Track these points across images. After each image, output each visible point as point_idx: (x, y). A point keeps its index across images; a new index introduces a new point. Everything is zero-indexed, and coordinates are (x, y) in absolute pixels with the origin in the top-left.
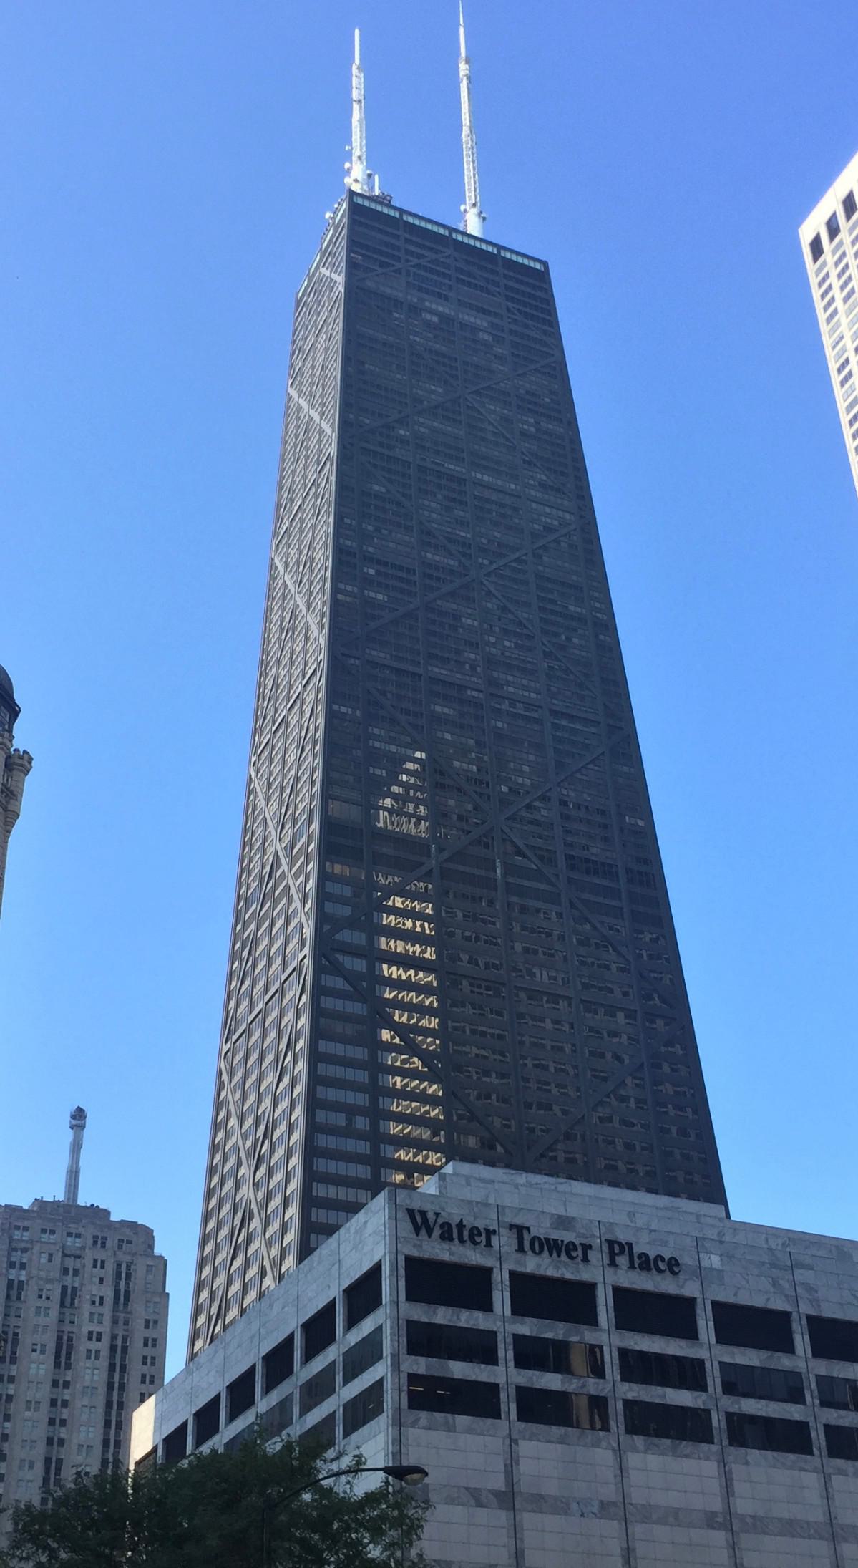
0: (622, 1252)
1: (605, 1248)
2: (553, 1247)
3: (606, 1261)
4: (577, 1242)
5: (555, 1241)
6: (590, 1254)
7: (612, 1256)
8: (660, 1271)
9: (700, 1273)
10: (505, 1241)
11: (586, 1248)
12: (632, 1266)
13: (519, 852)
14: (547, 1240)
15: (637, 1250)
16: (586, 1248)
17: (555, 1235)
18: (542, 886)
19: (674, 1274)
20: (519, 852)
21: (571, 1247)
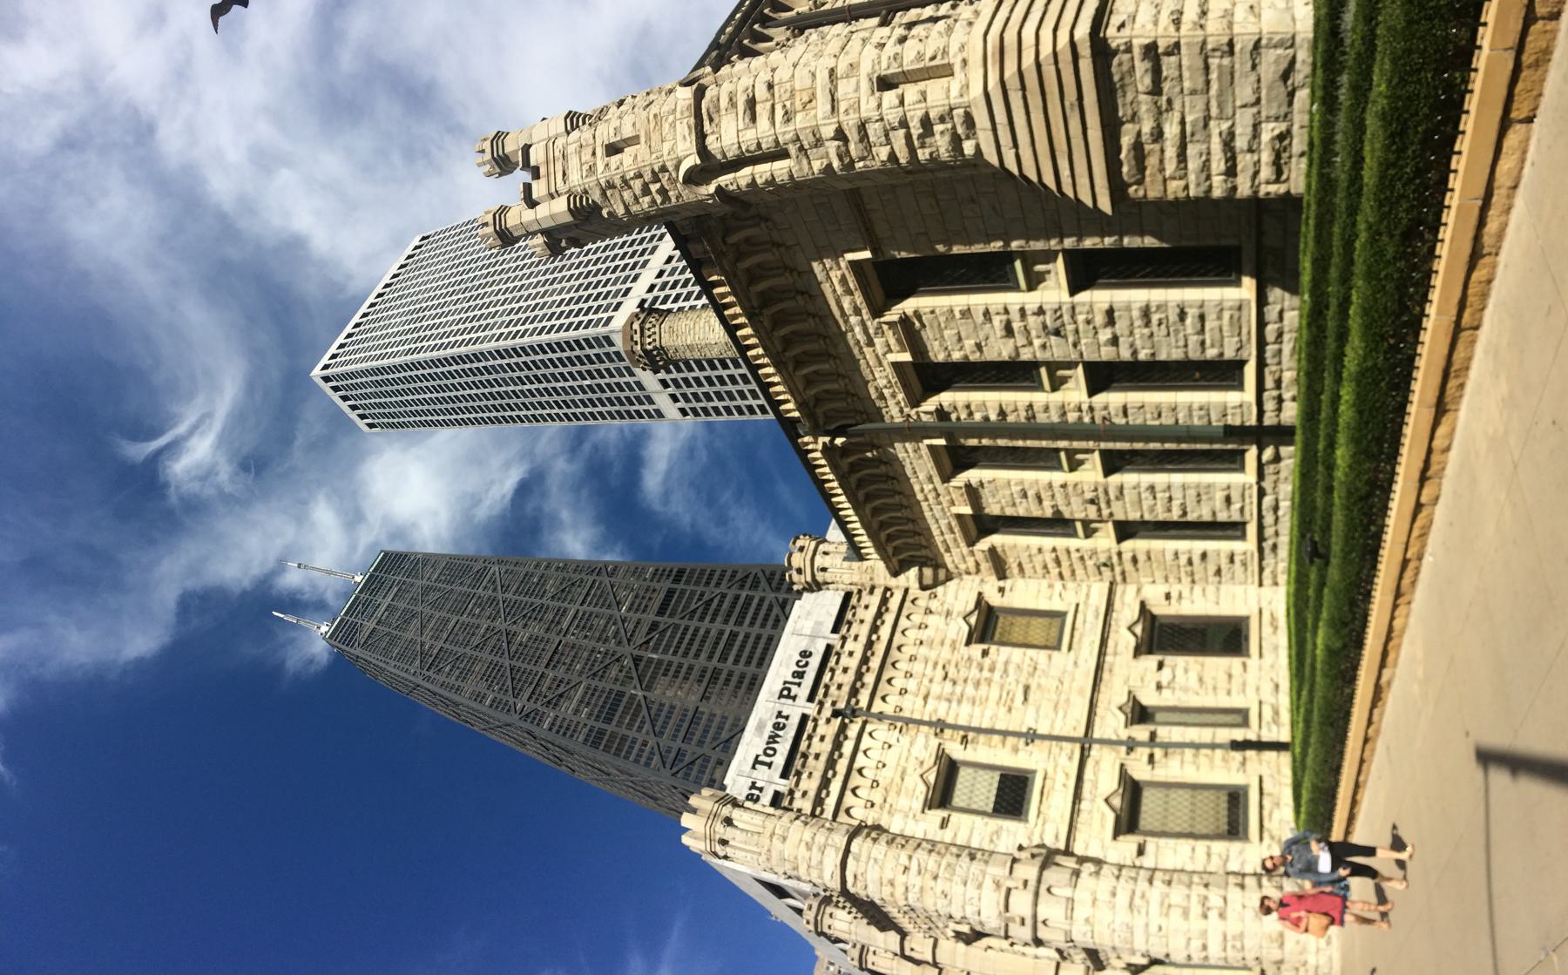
0: (789, 690)
1: (783, 700)
2: (773, 739)
3: (790, 701)
4: (774, 721)
5: (770, 737)
6: (784, 714)
7: (788, 697)
8: (807, 664)
9: (813, 637)
10: (762, 774)
11: (779, 715)
12: (799, 685)
13: (647, 642)
14: (768, 743)
15: (790, 679)
16: (779, 715)
17: (766, 737)
18: (669, 633)
19: (811, 654)
20: (647, 642)
21: (777, 726)
